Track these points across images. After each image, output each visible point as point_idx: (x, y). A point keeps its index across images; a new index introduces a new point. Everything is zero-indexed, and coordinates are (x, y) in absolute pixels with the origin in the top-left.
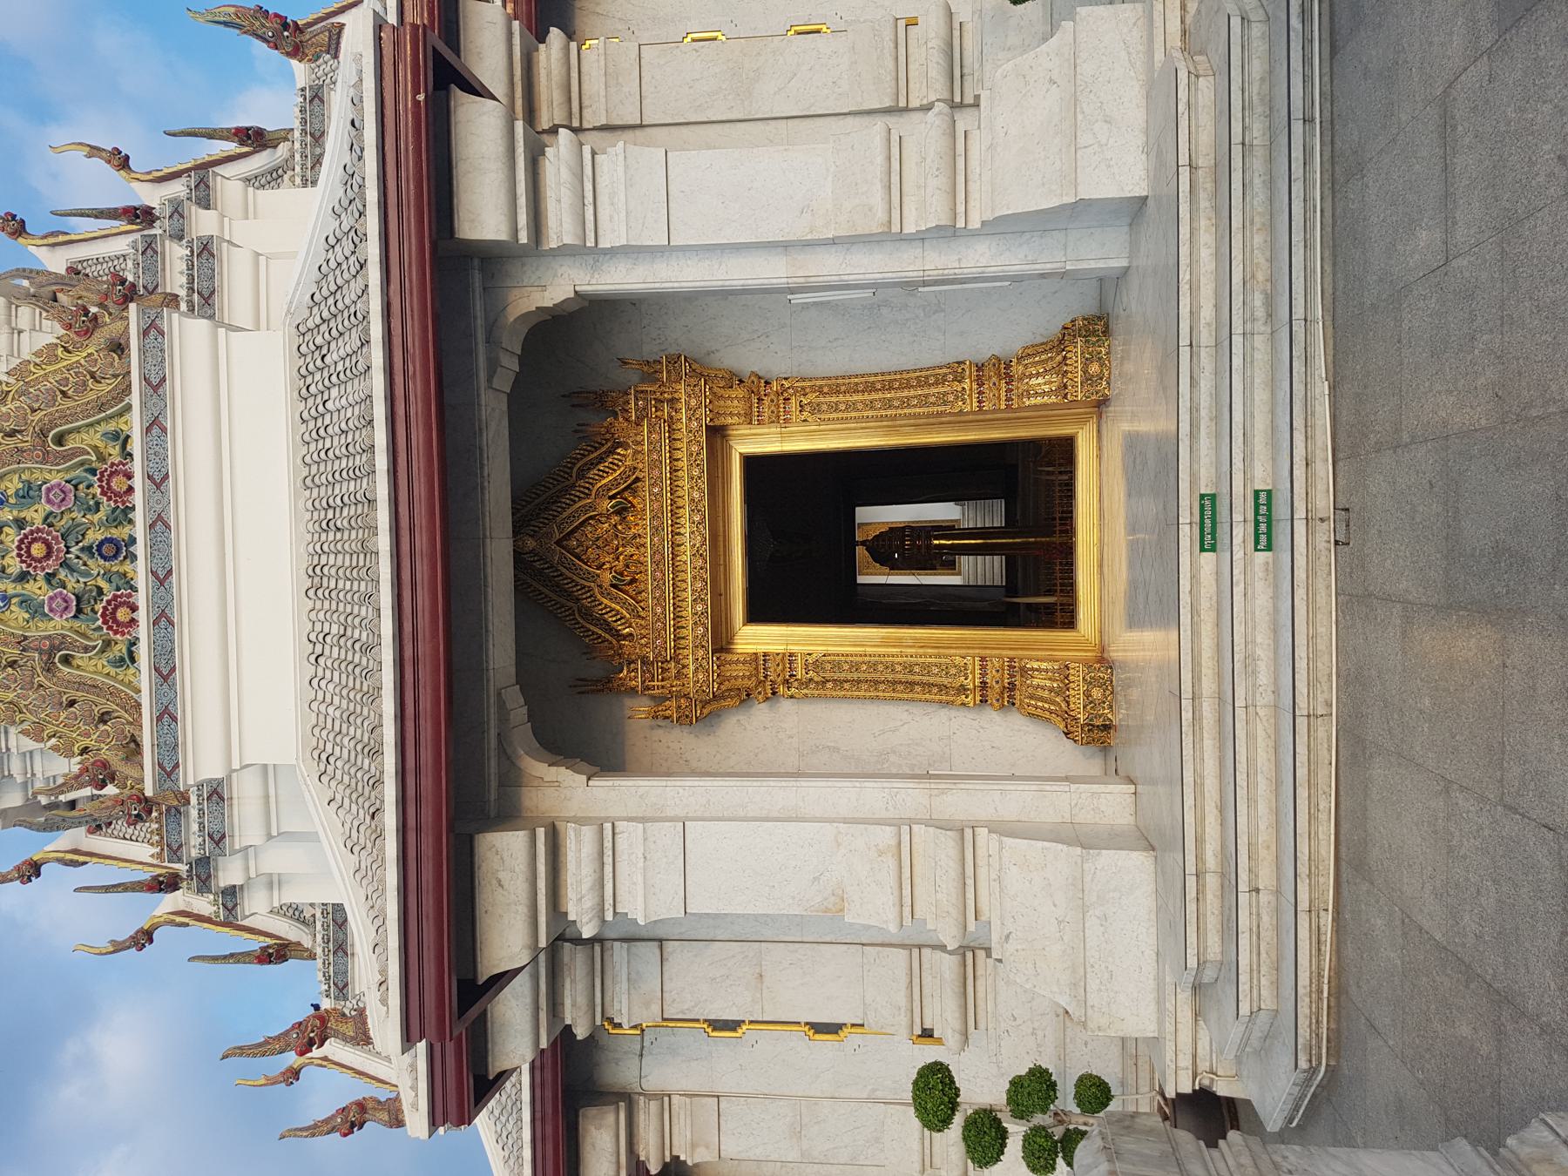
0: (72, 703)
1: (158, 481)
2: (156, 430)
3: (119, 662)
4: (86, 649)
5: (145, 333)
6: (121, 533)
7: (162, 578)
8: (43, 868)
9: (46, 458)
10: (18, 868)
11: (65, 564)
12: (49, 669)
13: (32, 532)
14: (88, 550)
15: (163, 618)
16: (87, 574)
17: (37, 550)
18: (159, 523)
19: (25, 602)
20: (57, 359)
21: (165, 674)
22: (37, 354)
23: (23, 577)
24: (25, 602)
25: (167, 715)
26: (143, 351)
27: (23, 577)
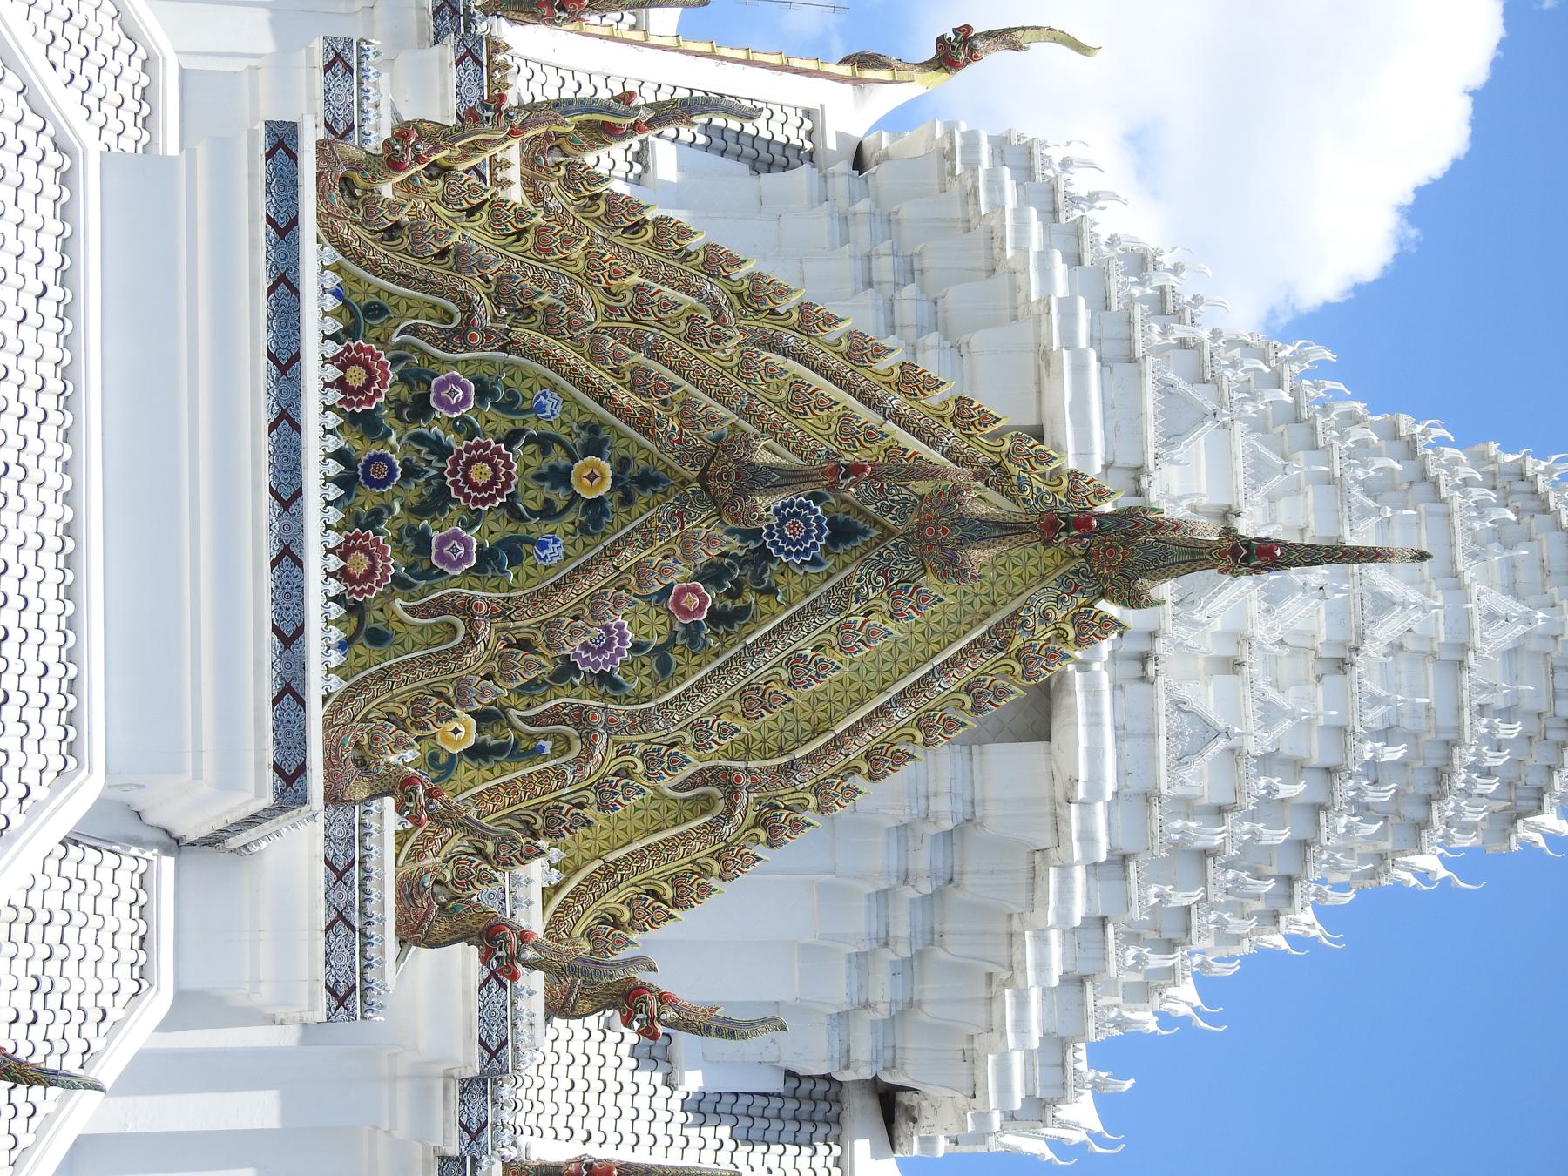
0: (443, 253)
1: (288, 557)
2: (288, 631)
3: (375, 311)
4: (414, 330)
5: (302, 769)
6: (367, 499)
7: (286, 421)
8: (930, 52)
9: (466, 608)
10: (973, 56)
11: (441, 450)
12: (467, 304)
13: (492, 498)
14: (410, 471)
15: (286, 363)
16: (419, 438)
17: (480, 474)
18: (288, 498)
19: (510, 404)
20: (676, 881)
21: (284, 284)
22: (705, 891)
23: (511, 439)
24: (510, 404)
25: (284, 228)
26: (302, 742)
27: (511, 439)
